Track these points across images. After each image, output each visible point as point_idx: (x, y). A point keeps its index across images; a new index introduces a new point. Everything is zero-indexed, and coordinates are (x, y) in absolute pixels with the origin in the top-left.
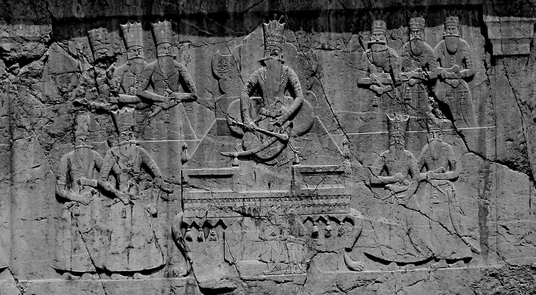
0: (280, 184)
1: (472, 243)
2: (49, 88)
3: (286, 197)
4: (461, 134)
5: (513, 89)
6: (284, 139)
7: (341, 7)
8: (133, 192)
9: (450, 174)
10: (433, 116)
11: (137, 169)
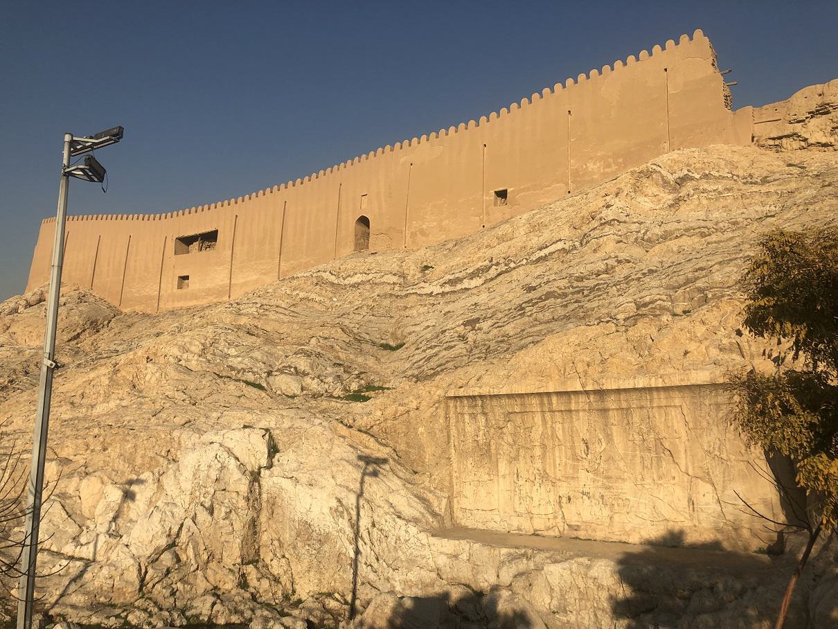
1: (685, 515)
2: (510, 440)
8: (541, 482)
9: (672, 482)
10: (662, 455)
11: (542, 472)
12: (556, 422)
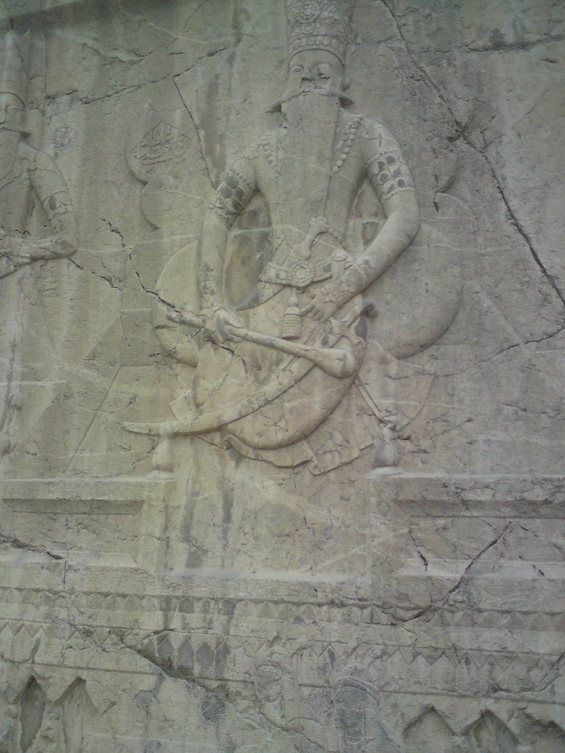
0: (317, 546)
3: (332, 603)
6: (337, 366)
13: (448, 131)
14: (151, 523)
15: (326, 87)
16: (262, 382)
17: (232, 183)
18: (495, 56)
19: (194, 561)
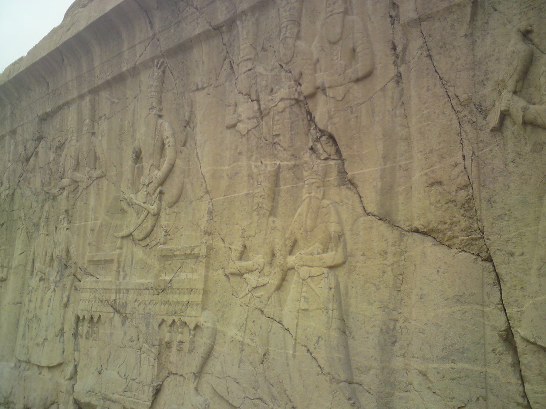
4: (352, 183)
5: (441, 78)
7: (207, 27)
10: (307, 156)
11: (64, 256)
12: (100, 118)
13: (184, 124)
14: (115, 266)
15: (155, 111)
16: (139, 218)
17: (134, 149)
18: (197, 93)
19: (124, 278)
